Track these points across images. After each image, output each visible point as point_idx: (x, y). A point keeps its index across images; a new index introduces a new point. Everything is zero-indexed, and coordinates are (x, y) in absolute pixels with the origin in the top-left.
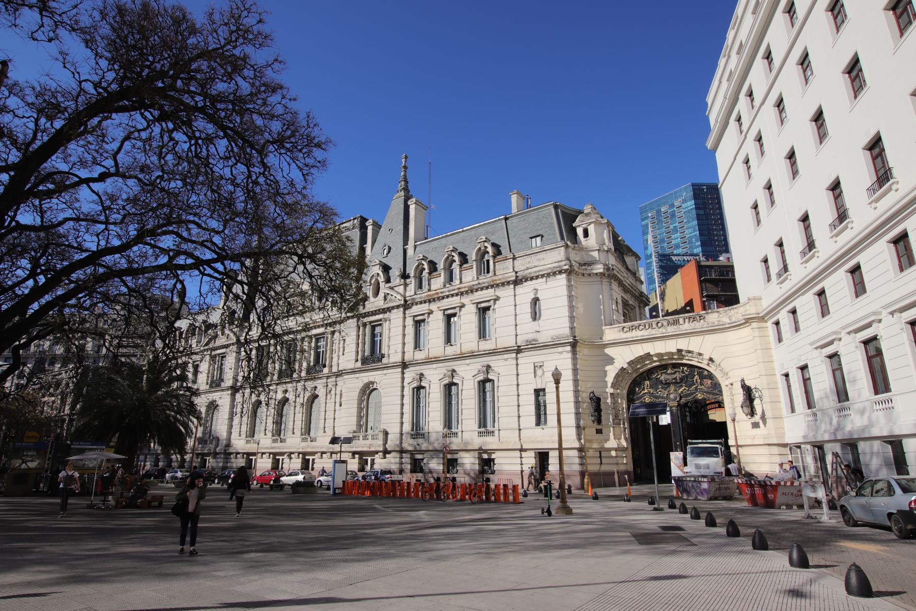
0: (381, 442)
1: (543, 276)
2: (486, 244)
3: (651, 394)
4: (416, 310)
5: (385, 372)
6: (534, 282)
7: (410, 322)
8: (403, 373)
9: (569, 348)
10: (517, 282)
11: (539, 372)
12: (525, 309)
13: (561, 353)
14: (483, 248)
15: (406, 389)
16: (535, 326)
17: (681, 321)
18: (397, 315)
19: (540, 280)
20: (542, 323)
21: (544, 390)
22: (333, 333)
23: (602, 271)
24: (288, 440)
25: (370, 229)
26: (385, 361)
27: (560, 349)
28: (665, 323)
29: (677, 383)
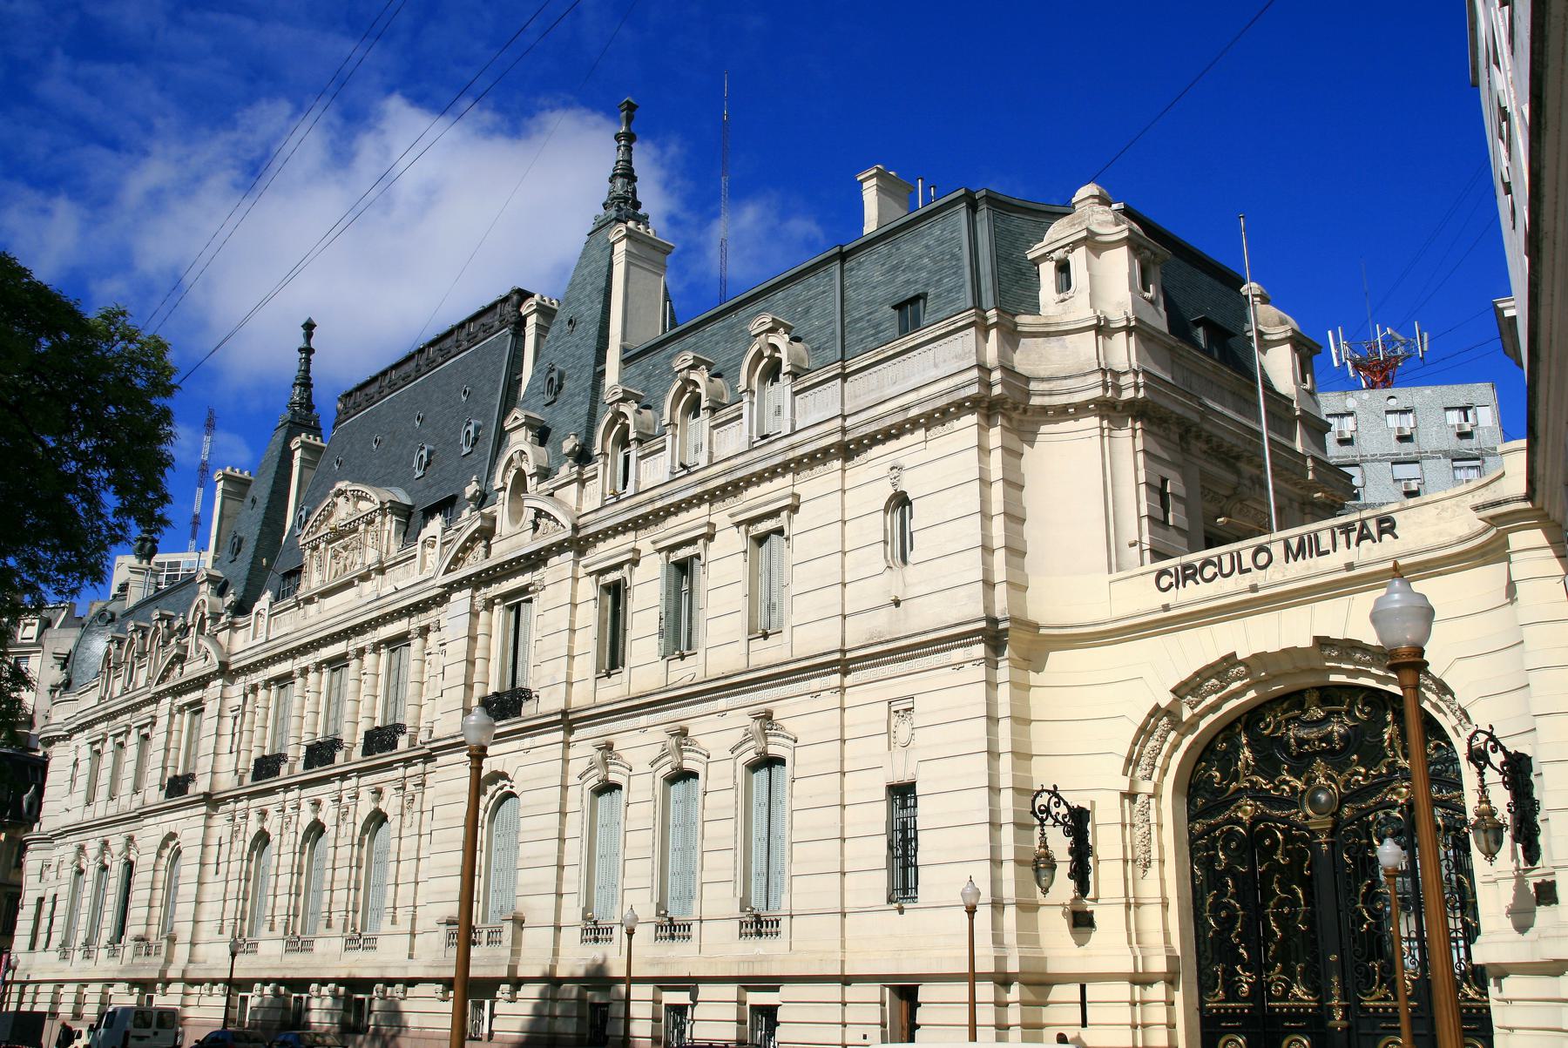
0: (504, 951)
1: (915, 424)
2: (773, 339)
3: (1257, 794)
4: (604, 552)
5: (527, 742)
6: (892, 445)
7: (588, 589)
8: (567, 745)
9: (979, 650)
10: (848, 450)
11: (903, 731)
12: (873, 526)
13: (958, 666)
14: (767, 353)
15: (573, 793)
16: (892, 584)
17: (1325, 541)
18: (561, 565)
19: (907, 439)
20: (915, 578)
21: (911, 787)
22: (424, 631)
23: (1098, 392)
24: (319, 945)
25: (532, 321)
26: (528, 709)
27: (957, 655)
28: (1278, 550)
29: (1332, 752)
